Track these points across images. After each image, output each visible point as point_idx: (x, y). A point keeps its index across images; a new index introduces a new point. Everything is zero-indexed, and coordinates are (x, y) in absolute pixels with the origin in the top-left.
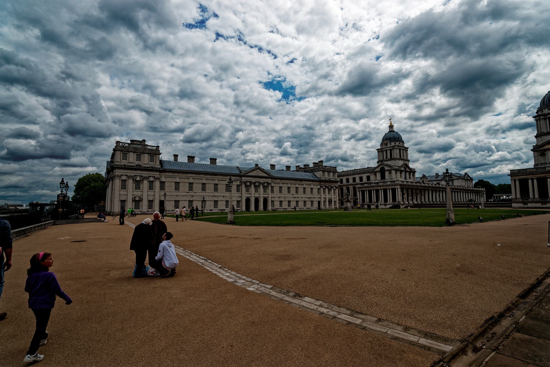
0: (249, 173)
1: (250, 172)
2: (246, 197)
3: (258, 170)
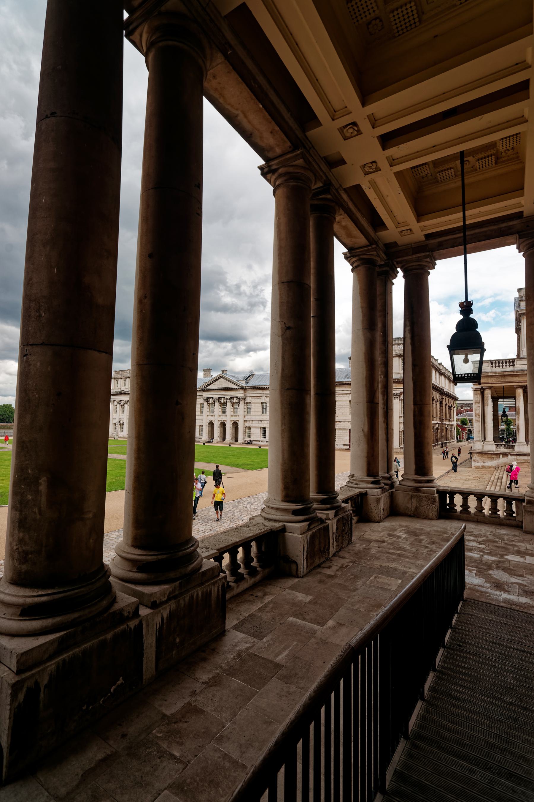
0: (209, 385)
1: (211, 384)
2: (209, 421)
3: (221, 379)
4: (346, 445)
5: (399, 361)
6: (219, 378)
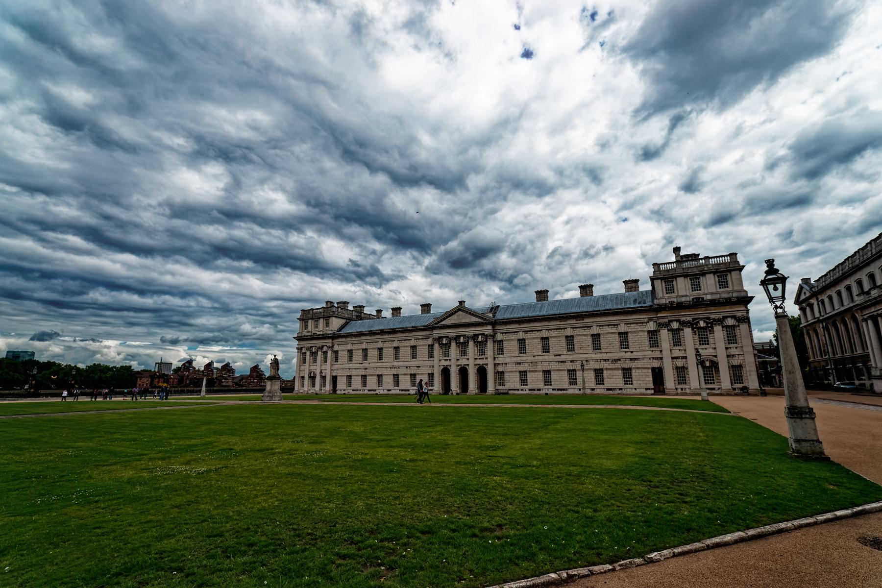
0: (442, 321)
1: (444, 319)
2: (442, 367)
3: (460, 313)
4: (649, 389)
5: (715, 277)
6: (456, 312)
